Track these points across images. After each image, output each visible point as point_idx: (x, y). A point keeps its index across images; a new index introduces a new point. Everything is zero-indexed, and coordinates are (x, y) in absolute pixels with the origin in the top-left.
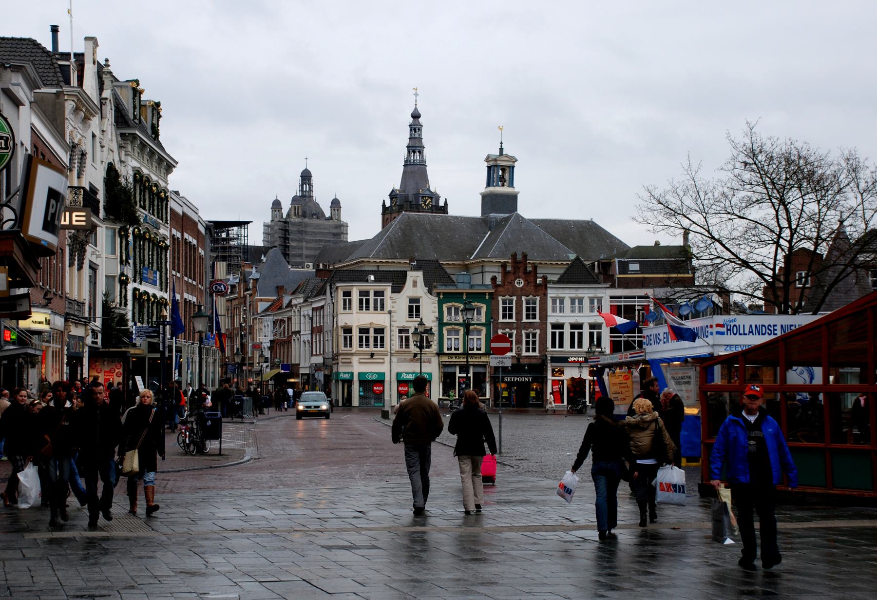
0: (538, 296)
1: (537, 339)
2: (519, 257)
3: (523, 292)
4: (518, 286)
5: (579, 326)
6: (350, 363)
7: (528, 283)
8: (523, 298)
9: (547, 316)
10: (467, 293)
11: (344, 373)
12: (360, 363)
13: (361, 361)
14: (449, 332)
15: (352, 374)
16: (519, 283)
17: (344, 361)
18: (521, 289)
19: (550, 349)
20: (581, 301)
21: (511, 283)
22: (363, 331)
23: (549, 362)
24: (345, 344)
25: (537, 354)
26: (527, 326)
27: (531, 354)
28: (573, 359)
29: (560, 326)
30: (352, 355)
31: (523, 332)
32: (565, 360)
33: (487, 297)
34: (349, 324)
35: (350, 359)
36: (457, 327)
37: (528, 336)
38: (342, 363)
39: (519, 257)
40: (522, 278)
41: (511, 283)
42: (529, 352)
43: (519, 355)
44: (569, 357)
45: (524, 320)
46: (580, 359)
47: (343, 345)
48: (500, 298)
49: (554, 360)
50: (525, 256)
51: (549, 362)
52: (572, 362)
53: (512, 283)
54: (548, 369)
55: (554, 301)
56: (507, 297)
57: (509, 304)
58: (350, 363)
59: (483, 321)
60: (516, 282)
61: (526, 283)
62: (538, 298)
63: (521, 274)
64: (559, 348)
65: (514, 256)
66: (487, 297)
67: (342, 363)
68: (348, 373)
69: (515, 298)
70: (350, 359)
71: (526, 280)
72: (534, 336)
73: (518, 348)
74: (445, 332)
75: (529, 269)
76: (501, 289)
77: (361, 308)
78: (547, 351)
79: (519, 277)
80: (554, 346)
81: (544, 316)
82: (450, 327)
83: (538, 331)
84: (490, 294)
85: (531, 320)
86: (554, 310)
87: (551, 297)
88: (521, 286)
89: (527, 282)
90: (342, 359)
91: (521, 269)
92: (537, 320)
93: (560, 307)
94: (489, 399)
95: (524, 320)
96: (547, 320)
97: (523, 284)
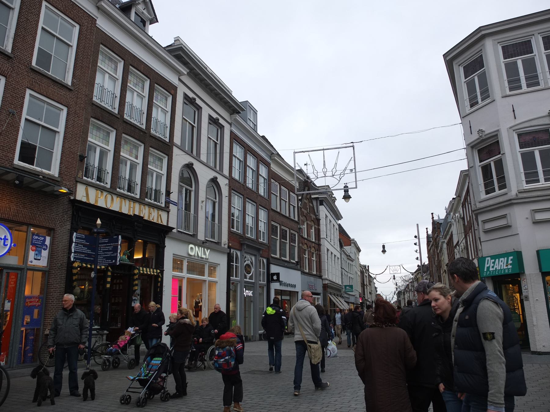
6: (508, 227)
11: (494, 257)
12: (536, 223)
13: (540, 216)
15: (518, 256)
17: (489, 226)
22: (528, 138)
24: (486, 186)
30: (509, 203)
34: (488, 130)
35: (504, 217)
38: (487, 232)
47: (482, 188)
58: (508, 227)
67: (487, 232)
68: (506, 255)
70: (504, 217)
77: (514, 84)
90: (484, 222)
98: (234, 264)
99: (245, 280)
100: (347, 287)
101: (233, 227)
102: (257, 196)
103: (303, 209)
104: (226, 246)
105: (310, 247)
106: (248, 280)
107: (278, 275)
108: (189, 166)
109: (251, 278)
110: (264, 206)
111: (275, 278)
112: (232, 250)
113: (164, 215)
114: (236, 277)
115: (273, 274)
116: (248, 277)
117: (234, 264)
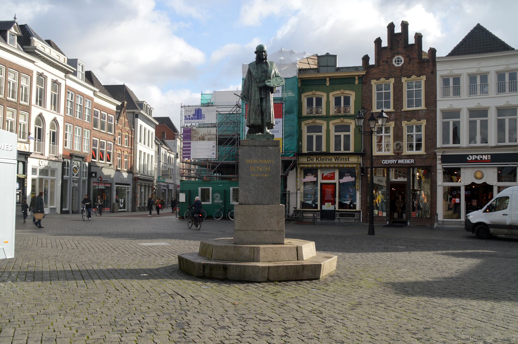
0: (423, 75)
1: (423, 133)
2: (398, 30)
3: (404, 72)
4: (396, 65)
5: (483, 112)
7: (410, 60)
8: (404, 80)
9: (436, 101)
10: (331, 79)
14: (310, 129)
16: (399, 61)
18: (401, 68)
19: (439, 144)
20: (484, 77)
21: (387, 62)
23: (439, 162)
25: (422, 152)
26: (408, 115)
27: (414, 152)
28: (474, 158)
29: (455, 113)
31: (404, 124)
32: (463, 159)
33: (357, 82)
36: (318, 121)
37: (410, 129)
39: (398, 30)
40: (402, 54)
41: (387, 62)
42: (413, 150)
43: (398, 154)
44: (468, 156)
45: (405, 108)
46: (485, 157)
48: (373, 82)
49: (445, 159)
50: (405, 26)
51: (439, 162)
52: (472, 161)
53: (389, 62)
54: (438, 171)
55: (446, 81)
56: (383, 79)
57: (385, 90)
59: (352, 112)
60: (394, 60)
61: (407, 60)
62: (424, 78)
63: (401, 50)
64: (454, 143)
65: (391, 27)
66: (357, 82)
69: (392, 81)
71: (406, 57)
72: (419, 129)
73: (397, 145)
74: (304, 129)
75: (411, 40)
76: (374, 71)
78: (436, 149)
79: (398, 54)
80: (445, 140)
81: (432, 101)
82: (310, 121)
83: (424, 122)
84: (361, 78)
85: (414, 108)
86: (446, 94)
87: (442, 76)
88: (400, 65)
89: (409, 59)
91: (401, 42)
92: (423, 107)
93: (454, 88)
94: (359, 212)
95: (405, 108)
96: (436, 107)
97: (403, 62)
98: (66, 168)
99: (73, 177)
100: (160, 178)
101: (66, 146)
102: (83, 123)
103: (119, 125)
104: (61, 158)
105: (123, 152)
106: (75, 177)
107: (96, 173)
108: (40, 115)
109: (77, 176)
110: (88, 128)
111: (94, 175)
112: (65, 160)
113: (27, 145)
114: (67, 175)
115: (93, 173)
116: (75, 175)
117: (66, 168)
